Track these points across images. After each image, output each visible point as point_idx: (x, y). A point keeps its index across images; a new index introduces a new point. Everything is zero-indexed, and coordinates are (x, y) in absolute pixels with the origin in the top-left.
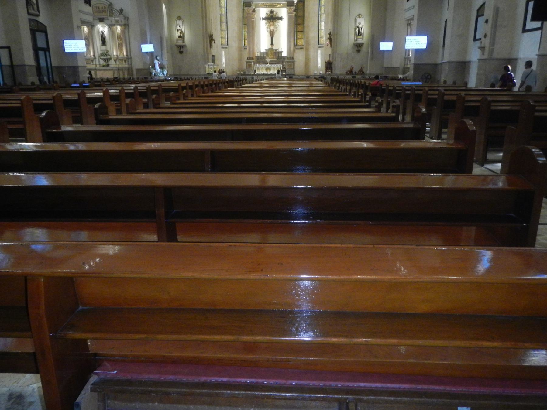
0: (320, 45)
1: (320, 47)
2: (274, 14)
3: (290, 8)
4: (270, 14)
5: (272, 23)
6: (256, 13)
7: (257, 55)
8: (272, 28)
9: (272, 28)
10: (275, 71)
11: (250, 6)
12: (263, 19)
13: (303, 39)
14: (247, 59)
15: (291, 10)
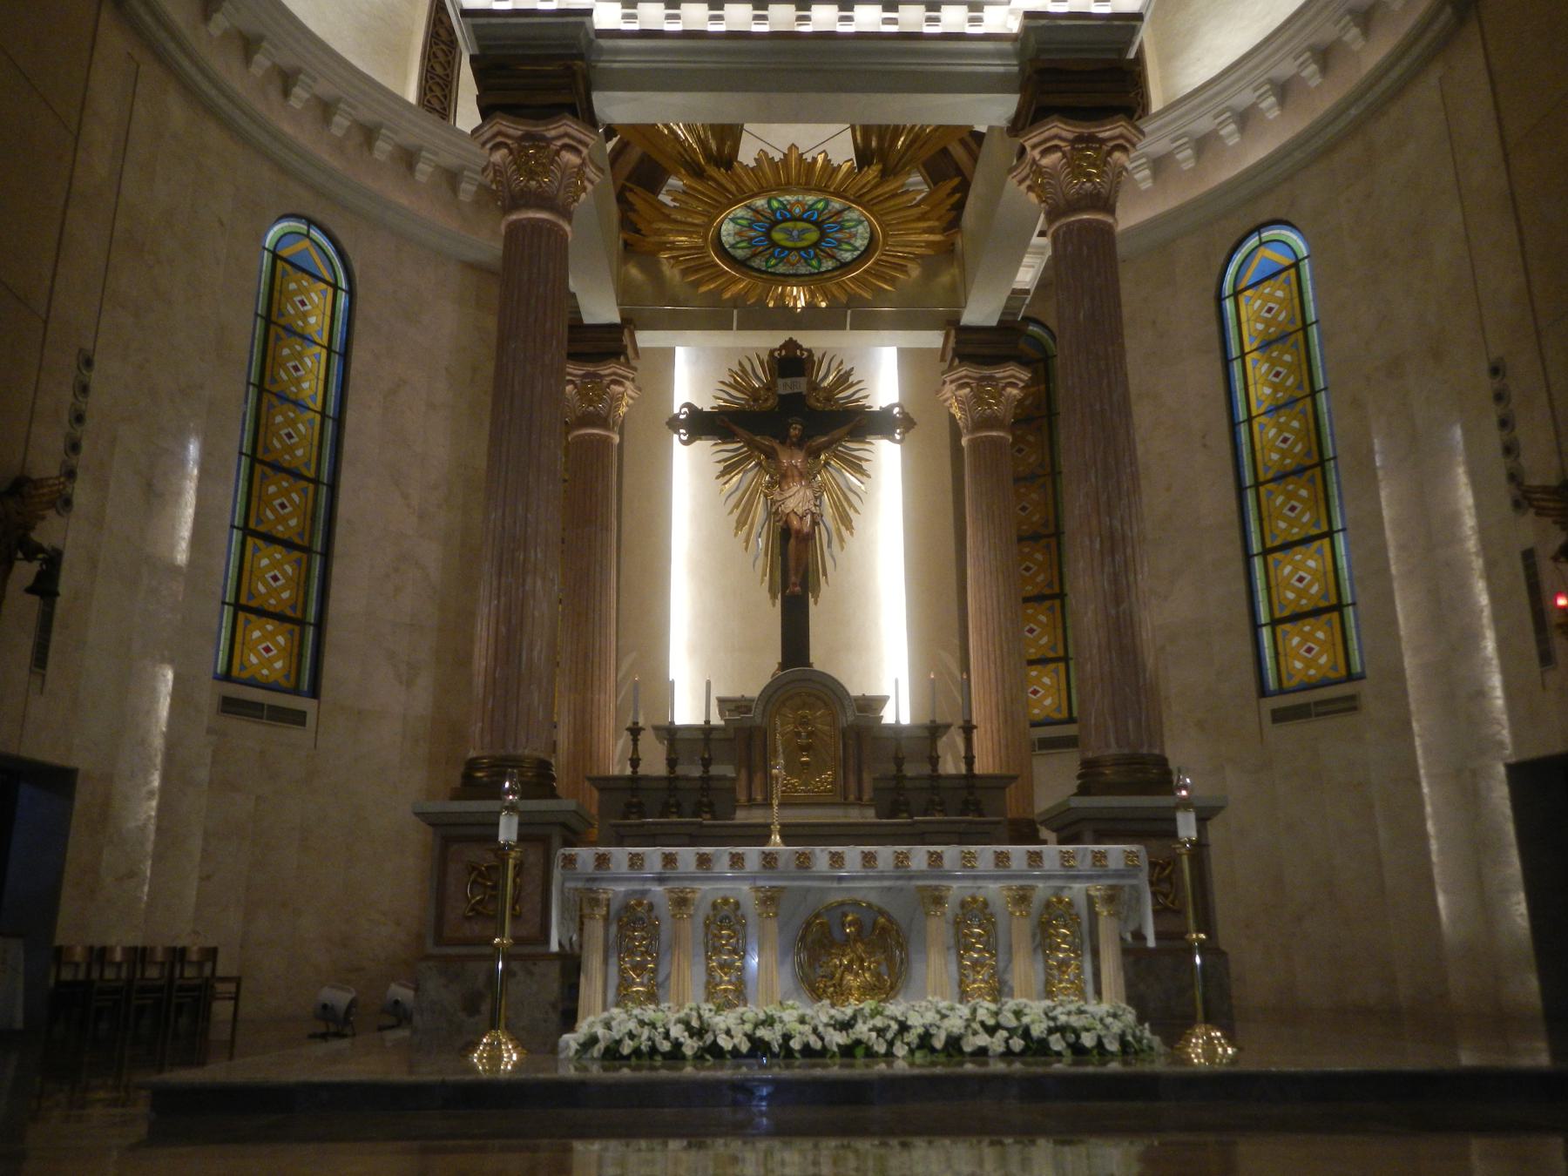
0: (1281, 691)
1: (1279, 716)
2: (814, 387)
3: (1090, 140)
4: (769, 387)
5: (794, 459)
6: (628, 364)
7: (617, 766)
8: (796, 499)
9: (796, 499)
10: (999, 991)
11: (550, 112)
12: (700, 424)
13: (1065, 659)
14: (468, 778)
15: (1102, 162)
